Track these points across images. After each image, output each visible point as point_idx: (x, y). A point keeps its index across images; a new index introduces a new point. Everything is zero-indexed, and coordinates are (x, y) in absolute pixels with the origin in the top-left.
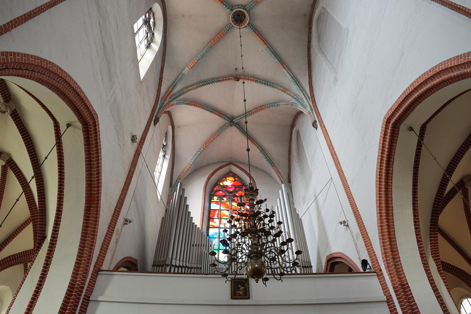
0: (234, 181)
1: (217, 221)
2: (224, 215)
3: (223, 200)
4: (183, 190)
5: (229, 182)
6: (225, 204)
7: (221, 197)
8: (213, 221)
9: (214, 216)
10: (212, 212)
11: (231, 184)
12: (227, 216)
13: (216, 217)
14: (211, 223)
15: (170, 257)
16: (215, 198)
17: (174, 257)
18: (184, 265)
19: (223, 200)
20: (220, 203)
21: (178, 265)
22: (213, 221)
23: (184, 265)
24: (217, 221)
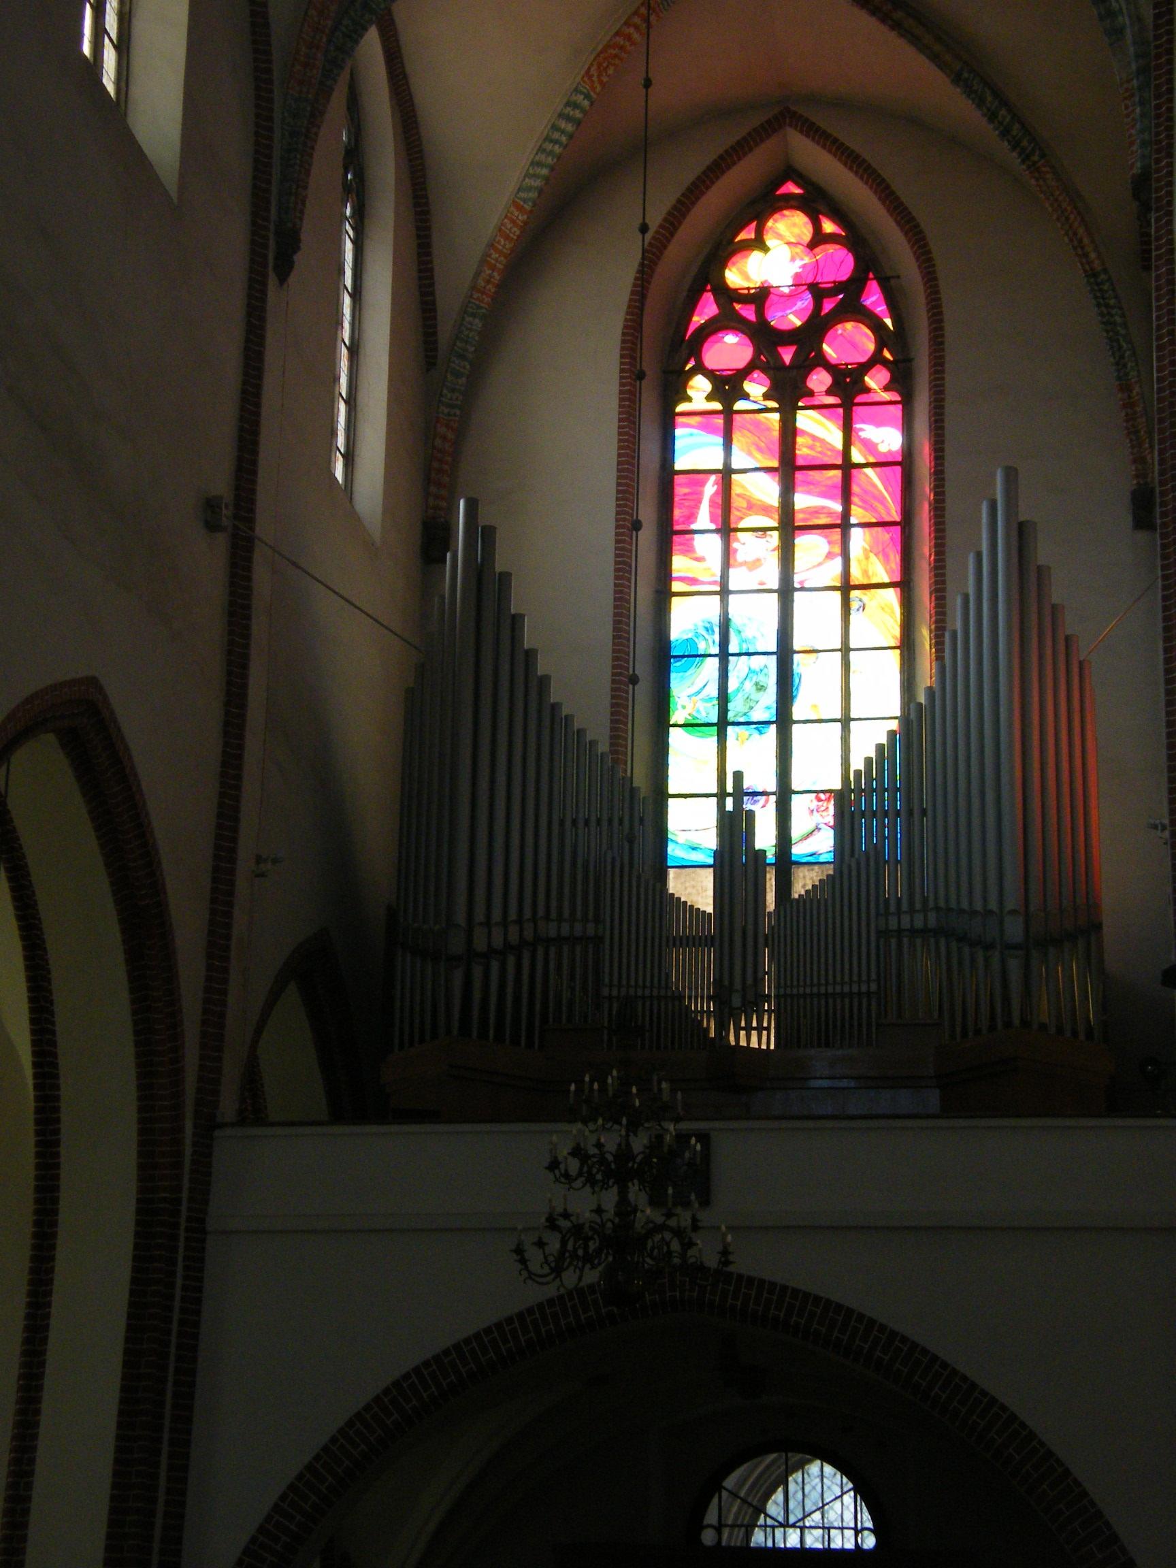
0: (812, 245)
1: (709, 545)
2: (753, 507)
3: (746, 397)
4: (489, 534)
5: (776, 260)
6: (759, 428)
7: (727, 387)
8: (689, 550)
9: (692, 517)
10: (681, 490)
11: (796, 267)
12: (765, 510)
13: (703, 519)
14: (680, 564)
15: (461, 918)
16: (699, 387)
17: (480, 916)
18: (529, 934)
19: (746, 397)
20: (719, 421)
21: (498, 942)
22: (689, 550)
23: (529, 934)
24: (709, 545)
